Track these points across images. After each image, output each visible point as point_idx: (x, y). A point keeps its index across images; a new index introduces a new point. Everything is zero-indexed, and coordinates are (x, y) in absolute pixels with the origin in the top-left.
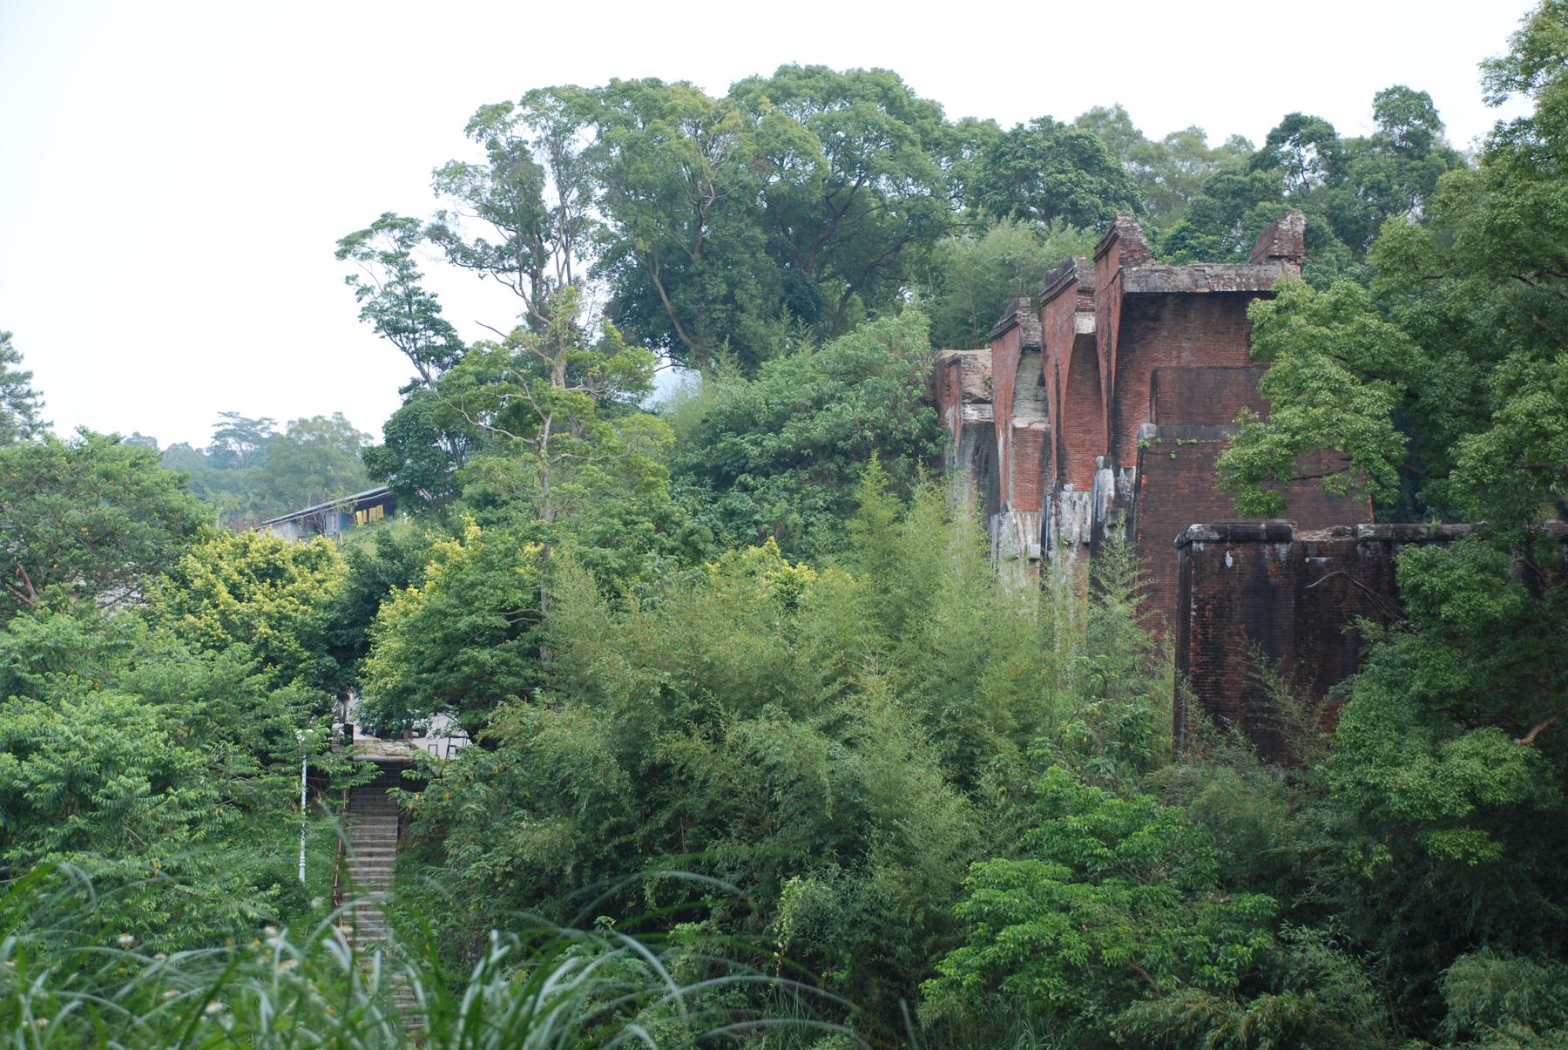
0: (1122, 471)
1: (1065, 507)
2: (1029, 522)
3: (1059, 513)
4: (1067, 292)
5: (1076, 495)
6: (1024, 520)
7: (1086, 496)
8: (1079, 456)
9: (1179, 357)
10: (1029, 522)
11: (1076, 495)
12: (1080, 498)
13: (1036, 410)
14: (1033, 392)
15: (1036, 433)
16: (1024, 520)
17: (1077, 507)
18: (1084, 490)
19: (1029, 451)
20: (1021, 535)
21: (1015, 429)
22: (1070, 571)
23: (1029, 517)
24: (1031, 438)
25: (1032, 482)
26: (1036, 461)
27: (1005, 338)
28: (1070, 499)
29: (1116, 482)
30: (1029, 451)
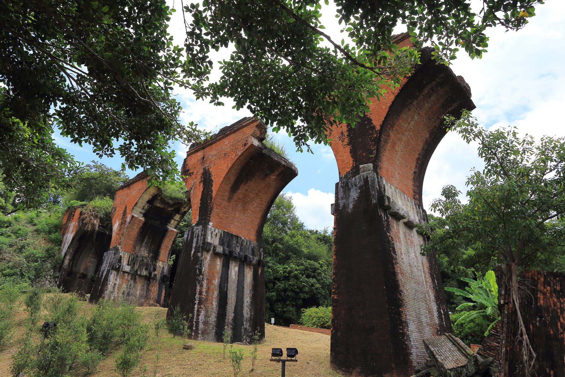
1: (209, 232)
6: (124, 254)
8: (217, 210)
12: (215, 231)
13: (141, 213)
14: (143, 205)
15: (140, 220)
16: (124, 254)
17: (213, 234)
19: (135, 227)
21: (133, 216)
23: (126, 254)
24: (137, 222)
25: (132, 240)
29: (378, 181)
30: (135, 227)
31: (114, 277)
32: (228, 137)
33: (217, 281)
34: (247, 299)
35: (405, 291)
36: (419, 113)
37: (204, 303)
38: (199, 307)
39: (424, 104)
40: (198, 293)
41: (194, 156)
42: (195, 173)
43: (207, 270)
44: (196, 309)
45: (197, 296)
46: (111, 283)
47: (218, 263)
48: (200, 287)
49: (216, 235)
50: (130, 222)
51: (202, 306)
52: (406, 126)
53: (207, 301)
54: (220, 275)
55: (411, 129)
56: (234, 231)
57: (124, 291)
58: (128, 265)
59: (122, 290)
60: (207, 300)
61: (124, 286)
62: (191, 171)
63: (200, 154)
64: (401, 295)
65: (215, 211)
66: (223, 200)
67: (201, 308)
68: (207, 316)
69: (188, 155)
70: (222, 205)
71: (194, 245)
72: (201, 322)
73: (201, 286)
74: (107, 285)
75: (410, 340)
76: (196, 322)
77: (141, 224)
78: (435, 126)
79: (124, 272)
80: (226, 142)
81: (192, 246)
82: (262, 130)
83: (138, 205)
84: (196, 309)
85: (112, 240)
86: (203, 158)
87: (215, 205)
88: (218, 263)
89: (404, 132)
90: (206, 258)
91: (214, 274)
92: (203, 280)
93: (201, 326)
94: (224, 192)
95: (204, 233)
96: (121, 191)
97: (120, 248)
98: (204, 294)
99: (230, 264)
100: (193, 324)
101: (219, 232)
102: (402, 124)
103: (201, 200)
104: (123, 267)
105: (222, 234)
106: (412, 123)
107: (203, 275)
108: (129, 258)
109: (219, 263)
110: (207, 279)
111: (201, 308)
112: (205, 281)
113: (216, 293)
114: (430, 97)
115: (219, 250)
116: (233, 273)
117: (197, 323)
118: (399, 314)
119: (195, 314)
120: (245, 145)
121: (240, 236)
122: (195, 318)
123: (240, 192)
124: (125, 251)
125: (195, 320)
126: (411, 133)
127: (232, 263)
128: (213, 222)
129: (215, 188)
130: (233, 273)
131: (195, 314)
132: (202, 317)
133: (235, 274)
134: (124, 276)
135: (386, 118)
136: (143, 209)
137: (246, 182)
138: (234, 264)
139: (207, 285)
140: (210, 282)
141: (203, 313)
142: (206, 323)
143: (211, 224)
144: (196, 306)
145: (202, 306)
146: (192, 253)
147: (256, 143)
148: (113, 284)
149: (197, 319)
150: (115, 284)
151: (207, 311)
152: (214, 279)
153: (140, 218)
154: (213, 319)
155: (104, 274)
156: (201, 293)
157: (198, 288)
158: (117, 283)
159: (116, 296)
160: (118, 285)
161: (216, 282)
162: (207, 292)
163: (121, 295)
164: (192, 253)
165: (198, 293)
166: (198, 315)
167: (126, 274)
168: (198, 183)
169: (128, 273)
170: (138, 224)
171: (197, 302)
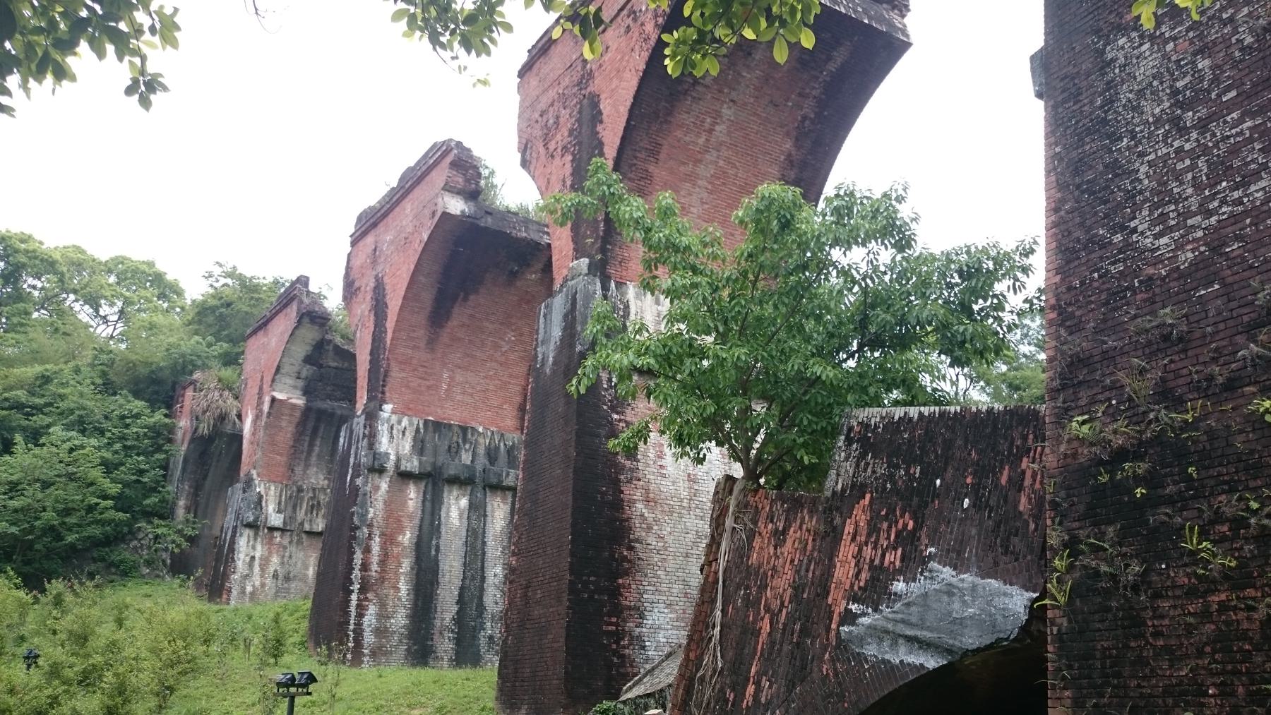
0: (613, 285)
1: (383, 429)
2: (272, 493)
3: (372, 437)
4: (439, 168)
5: (394, 418)
7: (405, 422)
8: (404, 375)
9: (711, 131)
10: (272, 493)
11: (394, 418)
12: (399, 422)
13: (295, 387)
14: (296, 368)
15: (294, 406)
17: (395, 432)
18: (404, 414)
19: (284, 424)
20: (264, 504)
21: (273, 400)
22: (380, 505)
23: (273, 488)
24: (287, 411)
25: (281, 454)
26: (289, 435)
27: (269, 326)
28: (389, 420)
30: (284, 424)
31: (249, 541)
32: (410, 196)
33: (408, 535)
34: (495, 572)
35: (652, 540)
36: (732, 101)
37: (375, 588)
38: (362, 597)
39: (739, 74)
40: (357, 567)
41: (361, 244)
42: (362, 289)
43: (380, 514)
44: (354, 603)
45: (356, 574)
46: (242, 556)
47: (412, 495)
48: (363, 553)
49: (404, 433)
50: (269, 414)
51: (370, 595)
52: (701, 141)
53: (383, 582)
54: (417, 521)
55: (721, 144)
56: (454, 416)
57: (276, 571)
58: (279, 511)
59: (272, 569)
60: (382, 579)
61: (275, 560)
62: (357, 284)
63: (370, 240)
64: (631, 548)
65: (396, 374)
66: (414, 348)
67: (366, 599)
68: (383, 615)
69: (353, 244)
70: (414, 361)
71: (352, 460)
72: (368, 630)
73: (367, 550)
74: (233, 561)
75: (643, 647)
76: (354, 631)
77: (298, 414)
78: (805, 118)
79: (272, 529)
80: (408, 207)
81: (349, 463)
82: (467, 171)
83: (282, 371)
84: (354, 603)
85: (243, 457)
86: (375, 250)
87: (393, 364)
88: (412, 495)
89: (699, 156)
90: (377, 488)
91: (399, 521)
92: (370, 537)
93: (369, 638)
94: (414, 331)
95: (370, 432)
96: (261, 333)
97: (255, 476)
98: (375, 567)
99: (445, 494)
100: (348, 636)
101: (411, 424)
102: (687, 139)
103: (371, 354)
104: (266, 518)
105: (421, 426)
106: (718, 128)
107: (370, 526)
108: (281, 496)
109: (413, 495)
110: (382, 535)
111: (366, 599)
112: (377, 539)
113: (406, 565)
114: (750, 54)
115: (409, 465)
116: (454, 514)
117: (359, 633)
118: (616, 592)
119: (353, 614)
120: (434, 213)
121: (474, 424)
122: (352, 622)
123: (455, 323)
124: (269, 481)
125: (352, 627)
126: (725, 153)
127: (450, 492)
128: (394, 403)
129: (390, 324)
130: (454, 514)
131: (353, 614)
132: (370, 618)
133: (461, 516)
134: (272, 538)
135: (623, 139)
136: (298, 378)
137: (465, 299)
138: (455, 493)
139: (382, 548)
140: (389, 539)
141: (372, 610)
142: (380, 632)
143: (388, 407)
144: (354, 597)
145: (370, 595)
146: (349, 478)
147: (456, 206)
148: (248, 559)
149: (359, 624)
150: (253, 558)
151: (383, 606)
152: (401, 530)
153: (294, 401)
154: (400, 620)
155: (228, 538)
156: (365, 567)
157: (358, 558)
158: (258, 555)
159: (257, 583)
160: (261, 559)
161: (407, 538)
162: (383, 563)
163: (269, 581)
164: (349, 478)
165: (357, 567)
166: (360, 616)
167: (277, 534)
168: (367, 313)
169: (283, 530)
170: (291, 415)
171: (356, 587)
